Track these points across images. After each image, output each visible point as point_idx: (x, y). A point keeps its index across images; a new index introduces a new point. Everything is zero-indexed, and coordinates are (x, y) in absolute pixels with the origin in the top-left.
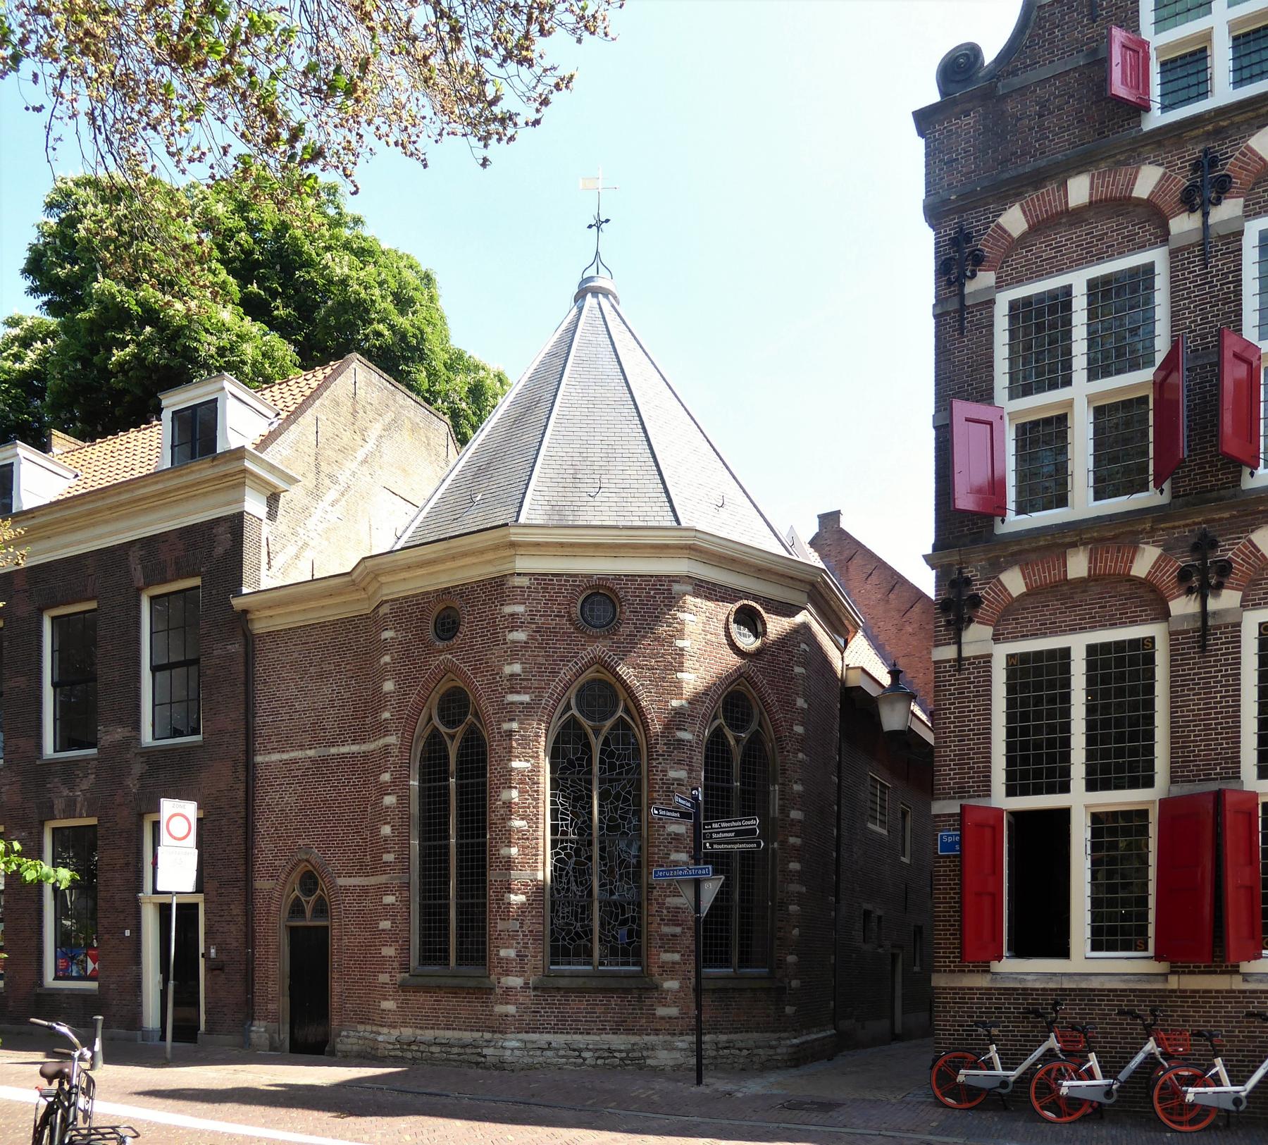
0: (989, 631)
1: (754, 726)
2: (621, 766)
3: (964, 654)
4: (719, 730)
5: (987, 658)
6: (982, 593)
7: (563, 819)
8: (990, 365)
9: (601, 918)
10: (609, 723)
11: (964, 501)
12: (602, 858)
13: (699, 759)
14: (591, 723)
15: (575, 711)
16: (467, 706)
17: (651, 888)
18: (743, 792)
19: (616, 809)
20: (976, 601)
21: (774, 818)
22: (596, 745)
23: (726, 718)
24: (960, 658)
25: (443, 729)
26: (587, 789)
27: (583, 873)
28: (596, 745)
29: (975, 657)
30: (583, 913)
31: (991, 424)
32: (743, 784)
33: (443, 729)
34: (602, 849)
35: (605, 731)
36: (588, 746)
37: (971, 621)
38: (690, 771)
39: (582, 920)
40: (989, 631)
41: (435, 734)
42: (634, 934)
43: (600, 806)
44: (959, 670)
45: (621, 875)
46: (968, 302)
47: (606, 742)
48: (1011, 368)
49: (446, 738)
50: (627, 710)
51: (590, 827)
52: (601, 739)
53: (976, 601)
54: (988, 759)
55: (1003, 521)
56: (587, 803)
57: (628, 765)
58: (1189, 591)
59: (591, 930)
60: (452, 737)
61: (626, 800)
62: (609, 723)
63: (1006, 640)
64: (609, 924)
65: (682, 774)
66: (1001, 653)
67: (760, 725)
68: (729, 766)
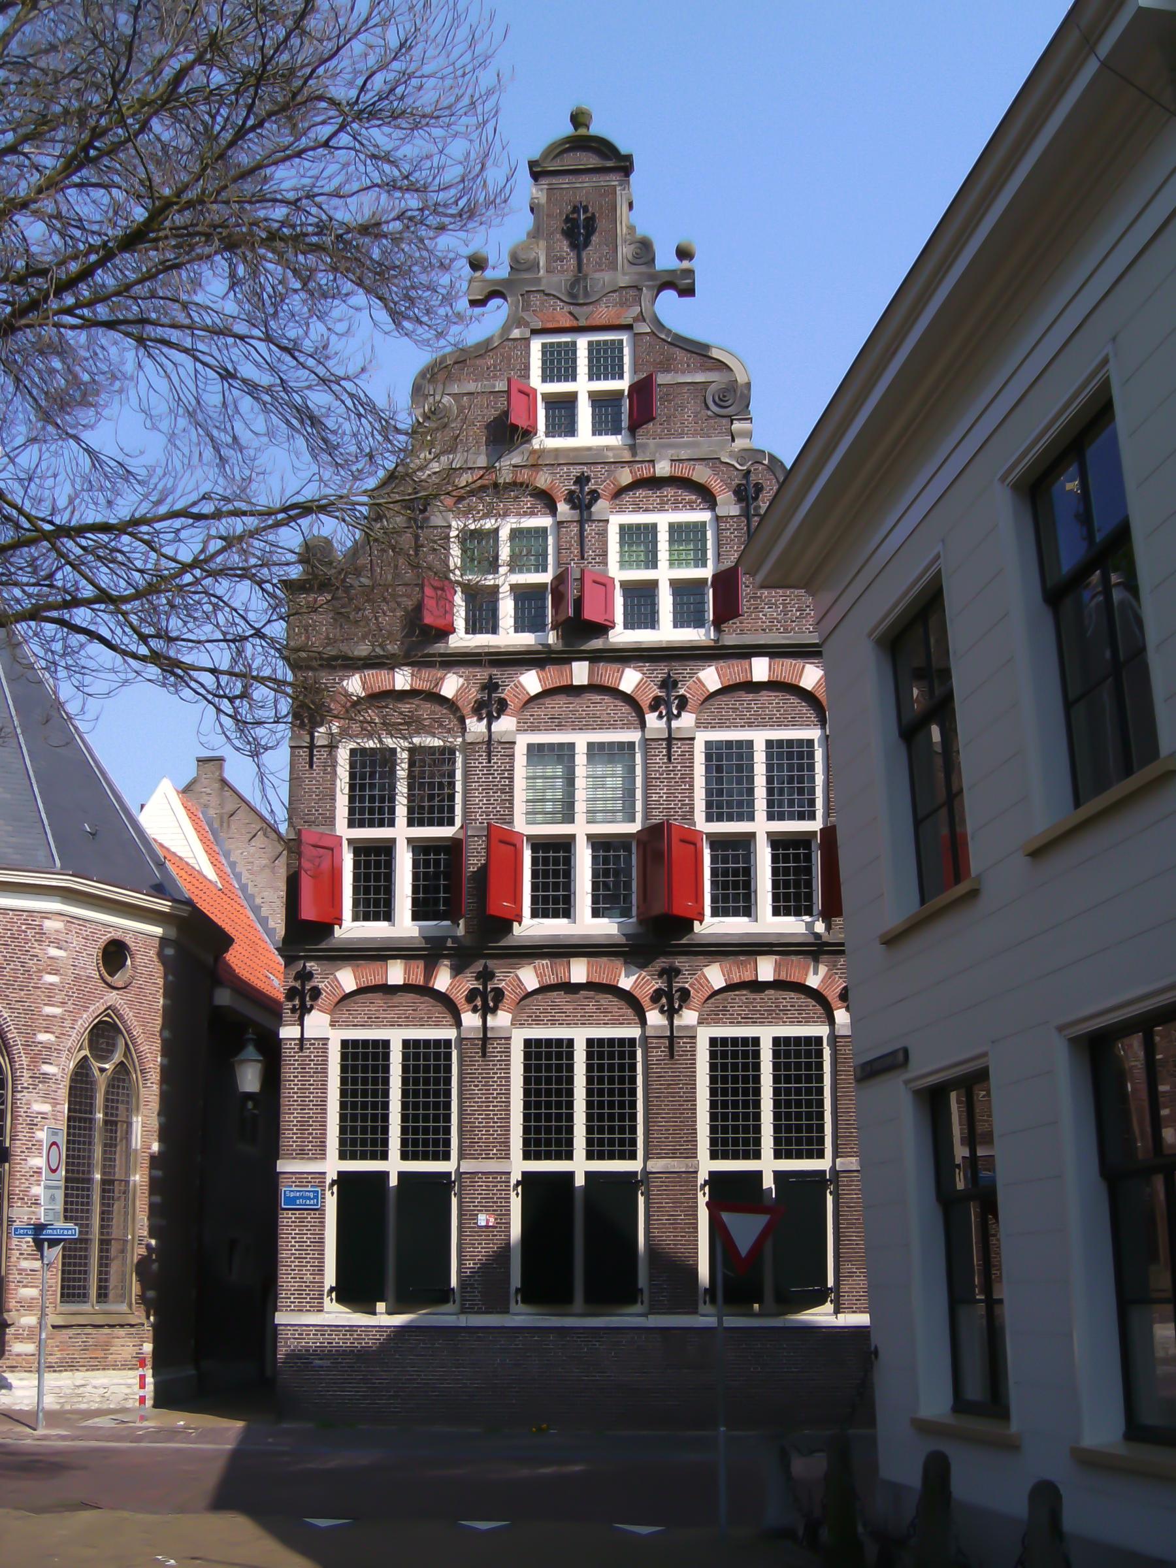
0: (327, 1018)
1: (118, 1057)
6: (321, 986)
11: (308, 912)
13: (63, 1093)
18: (106, 1122)
20: (316, 993)
21: (136, 1150)
24: (302, 1039)
29: (315, 1039)
32: (106, 1114)
37: (312, 1008)
38: (54, 1105)
40: (327, 1018)
53: (316, 993)
54: (324, 1125)
58: (475, 1010)
65: (46, 1108)
66: (336, 1038)
67: (125, 1055)
68: (92, 1097)
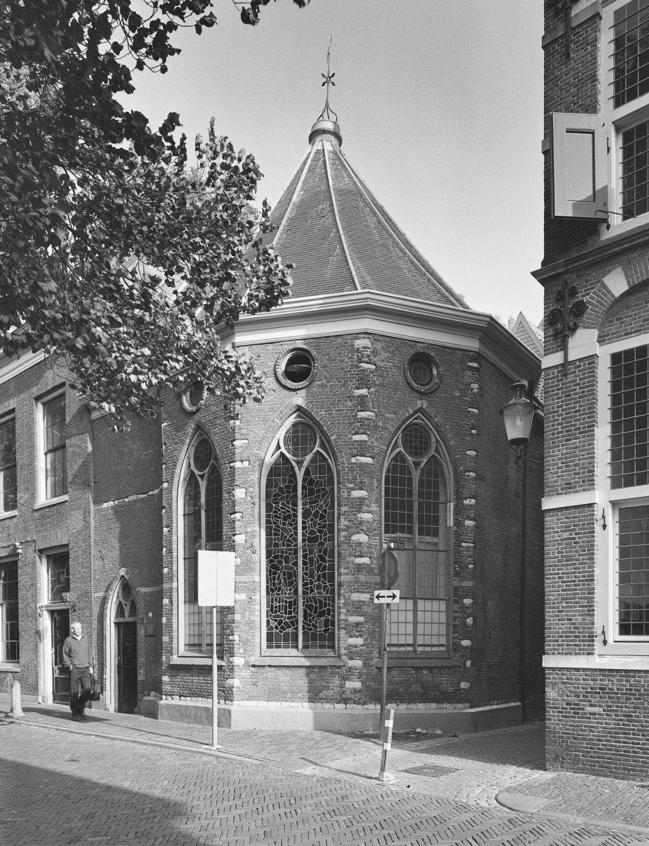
2: (318, 491)
3: (571, 358)
4: (400, 457)
5: (592, 359)
7: (275, 534)
8: (594, 79)
9: (305, 612)
10: (309, 457)
12: (304, 563)
14: (294, 458)
15: (283, 450)
16: (210, 454)
17: (340, 585)
19: (315, 524)
22: (300, 475)
23: (405, 448)
25: (197, 472)
26: (293, 510)
27: (290, 576)
28: (300, 475)
29: (581, 360)
30: (290, 607)
31: (593, 133)
33: (197, 472)
34: (305, 556)
35: (305, 464)
36: (294, 476)
39: (290, 613)
40: (595, 333)
41: (192, 473)
42: (330, 623)
43: (303, 522)
44: (566, 375)
45: (319, 576)
46: (574, 24)
47: (307, 472)
48: (616, 77)
49: (199, 479)
50: (322, 446)
51: (296, 540)
52: (303, 470)
53: (580, 309)
55: (608, 227)
56: (293, 521)
57: (324, 490)
59: (297, 621)
60: (202, 477)
61: (322, 517)
62: (309, 457)
63: (611, 341)
64: (311, 615)
